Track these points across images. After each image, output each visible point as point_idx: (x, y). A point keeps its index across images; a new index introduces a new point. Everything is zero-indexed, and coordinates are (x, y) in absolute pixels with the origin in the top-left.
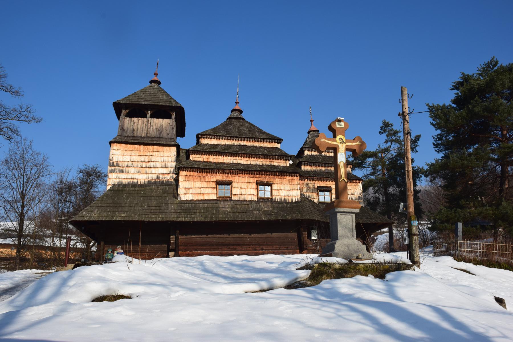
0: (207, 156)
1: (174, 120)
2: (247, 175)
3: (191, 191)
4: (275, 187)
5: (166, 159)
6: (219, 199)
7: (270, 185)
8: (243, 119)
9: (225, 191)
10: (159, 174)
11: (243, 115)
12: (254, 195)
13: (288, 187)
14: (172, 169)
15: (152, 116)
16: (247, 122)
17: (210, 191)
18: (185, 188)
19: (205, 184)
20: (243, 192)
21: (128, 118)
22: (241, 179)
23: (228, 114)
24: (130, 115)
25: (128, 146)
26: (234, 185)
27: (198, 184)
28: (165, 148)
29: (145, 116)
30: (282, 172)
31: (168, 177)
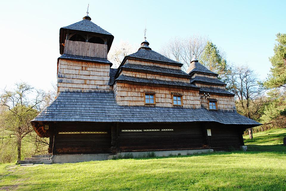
0: (135, 73)
1: (107, 45)
2: (164, 89)
3: (126, 99)
4: (184, 98)
5: (102, 74)
6: (146, 106)
7: (180, 96)
8: (150, 49)
9: (149, 100)
10: (98, 85)
11: (150, 46)
12: (170, 103)
13: (192, 98)
14: (108, 82)
15: (89, 42)
16: (153, 52)
17: (140, 99)
18: (121, 97)
19: (136, 94)
20: (163, 100)
21: (72, 41)
22: (161, 92)
23: (140, 46)
24: (73, 39)
25: (72, 63)
26: (157, 95)
27: (130, 94)
28: (101, 66)
29: (85, 41)
30: (187, 89)
31: (103, 87)
